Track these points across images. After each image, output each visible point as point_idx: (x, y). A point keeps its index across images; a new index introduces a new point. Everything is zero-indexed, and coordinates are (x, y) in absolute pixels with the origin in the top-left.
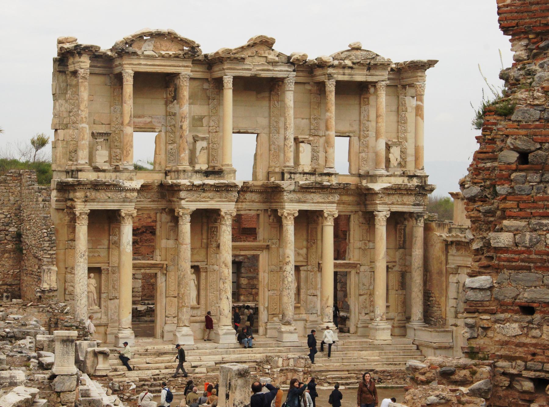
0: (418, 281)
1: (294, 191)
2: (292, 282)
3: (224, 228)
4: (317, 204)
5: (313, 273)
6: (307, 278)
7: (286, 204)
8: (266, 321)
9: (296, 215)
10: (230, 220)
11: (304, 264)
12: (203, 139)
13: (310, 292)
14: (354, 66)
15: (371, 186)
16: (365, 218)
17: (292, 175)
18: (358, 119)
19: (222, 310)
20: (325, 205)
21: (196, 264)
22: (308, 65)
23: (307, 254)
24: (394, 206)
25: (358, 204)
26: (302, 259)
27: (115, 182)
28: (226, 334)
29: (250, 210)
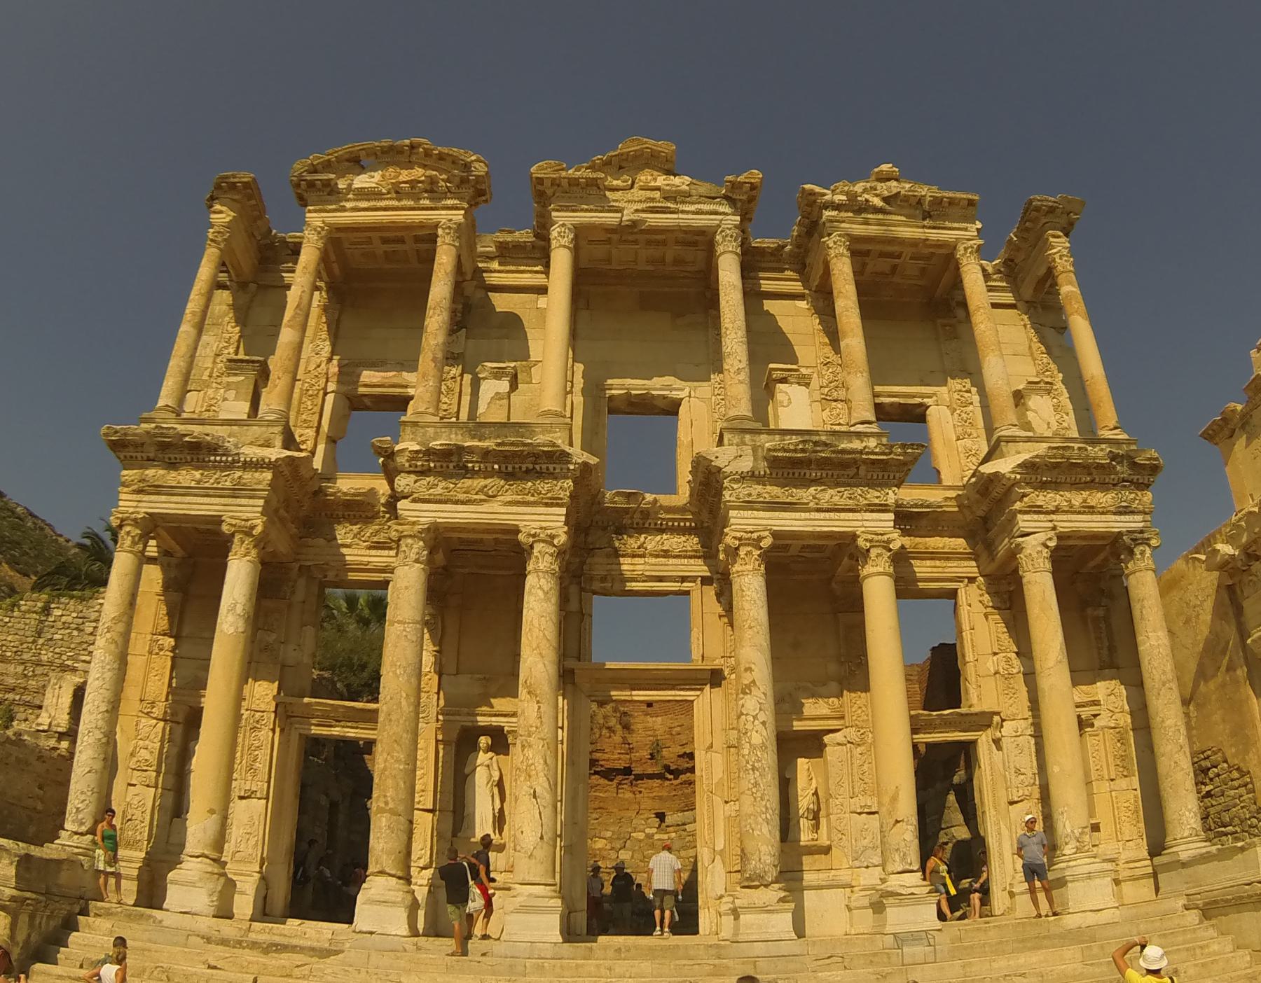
1: (752, 477)
2: (763, 746)
3: (531, 581)
7: (732, 513)
9: (766, 543)
12: (498, 375)
13: (857, 803)
14: (887, 207)
15: (988, 469)
17: (748, 437)
20: (858, 516)
21: (495, 721)
22: (791, 254)
25: (975, 556)
27: (209, 438)
28: (525, 909)
29: (660, 579)
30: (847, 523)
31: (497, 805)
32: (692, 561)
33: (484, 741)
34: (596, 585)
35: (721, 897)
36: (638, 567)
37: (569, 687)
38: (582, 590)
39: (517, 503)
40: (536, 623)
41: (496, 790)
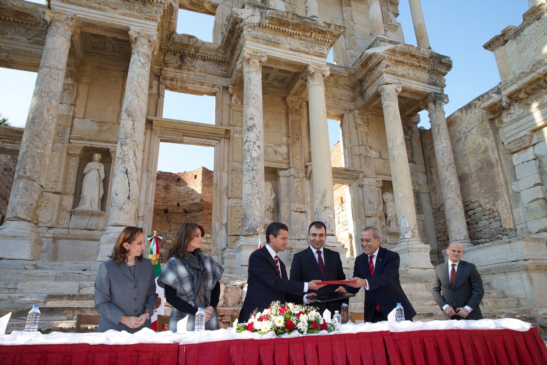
0: (452, 183)
2: (258, 158)
3: (134, 57)
4: (297, 53)
5: (298, 179)
6: (289, 185)
8: (224, 246)
9: (264, 59)
10: (146, 47)
11: (285, 166)
13: (294, 206)
16: (362, 119)
18: (340, 17)
19: (114, 195)
21: (104, 145)
23: (288, 154)
24: (405, 80)
25: (353, 100)
26: (280, 158)
30: (304, 59)
31: (102, 192)
32: (219, 78)
33: (97, 156)
34: (168, 82)
35: (225, 249)
36: (190, 76)
37: (149, 131)
38: (159, 83)
39: (130, 16)
40: (135, 78)
41: (102, 184)
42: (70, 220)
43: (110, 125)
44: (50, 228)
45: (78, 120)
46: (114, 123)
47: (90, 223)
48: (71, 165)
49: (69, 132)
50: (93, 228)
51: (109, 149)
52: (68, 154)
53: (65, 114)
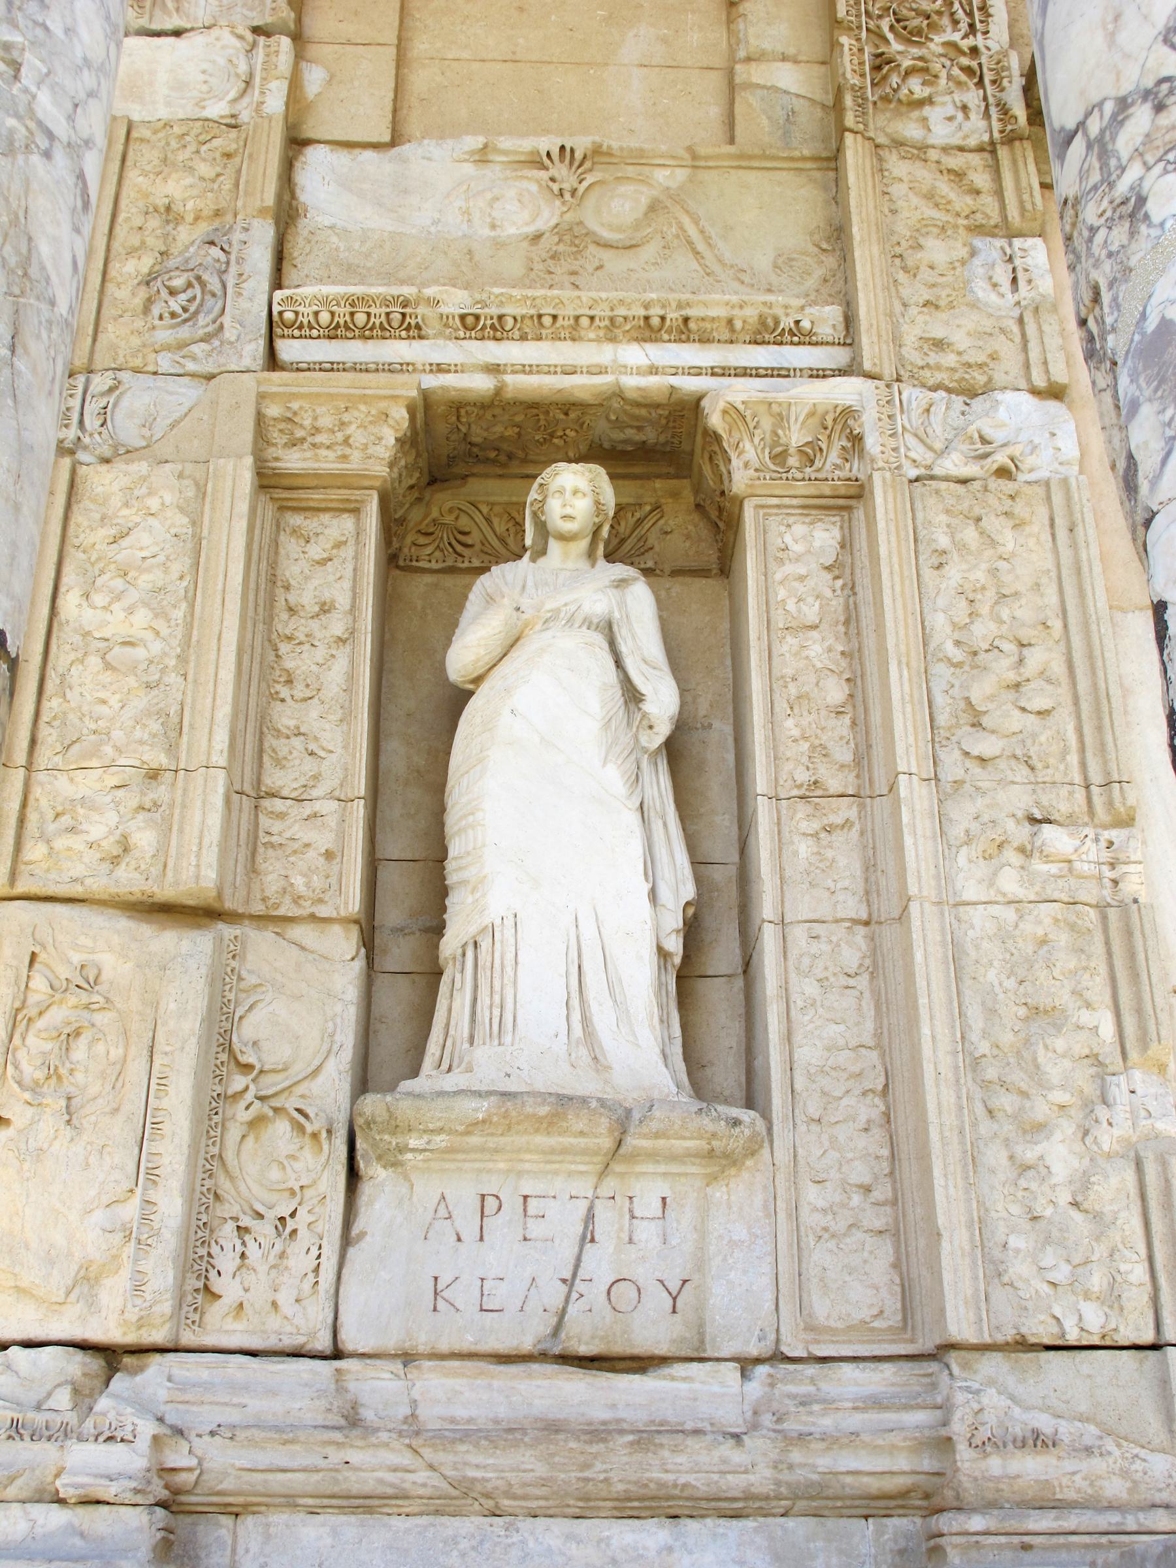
21: (638, 368)
31: (679, 887)
33: (573, 492)
41: (659, 786)
42: (347, 1240)
43: (661, 176)
44: (111, 1357)
45: (342, 158)
46: (695, 160)
47: (600, 1265)
48: (306, 598)
49: (261, 259)
50: (650, 1332)
51: (684, 413)
52: (268, 481)
53: (217, 109)
